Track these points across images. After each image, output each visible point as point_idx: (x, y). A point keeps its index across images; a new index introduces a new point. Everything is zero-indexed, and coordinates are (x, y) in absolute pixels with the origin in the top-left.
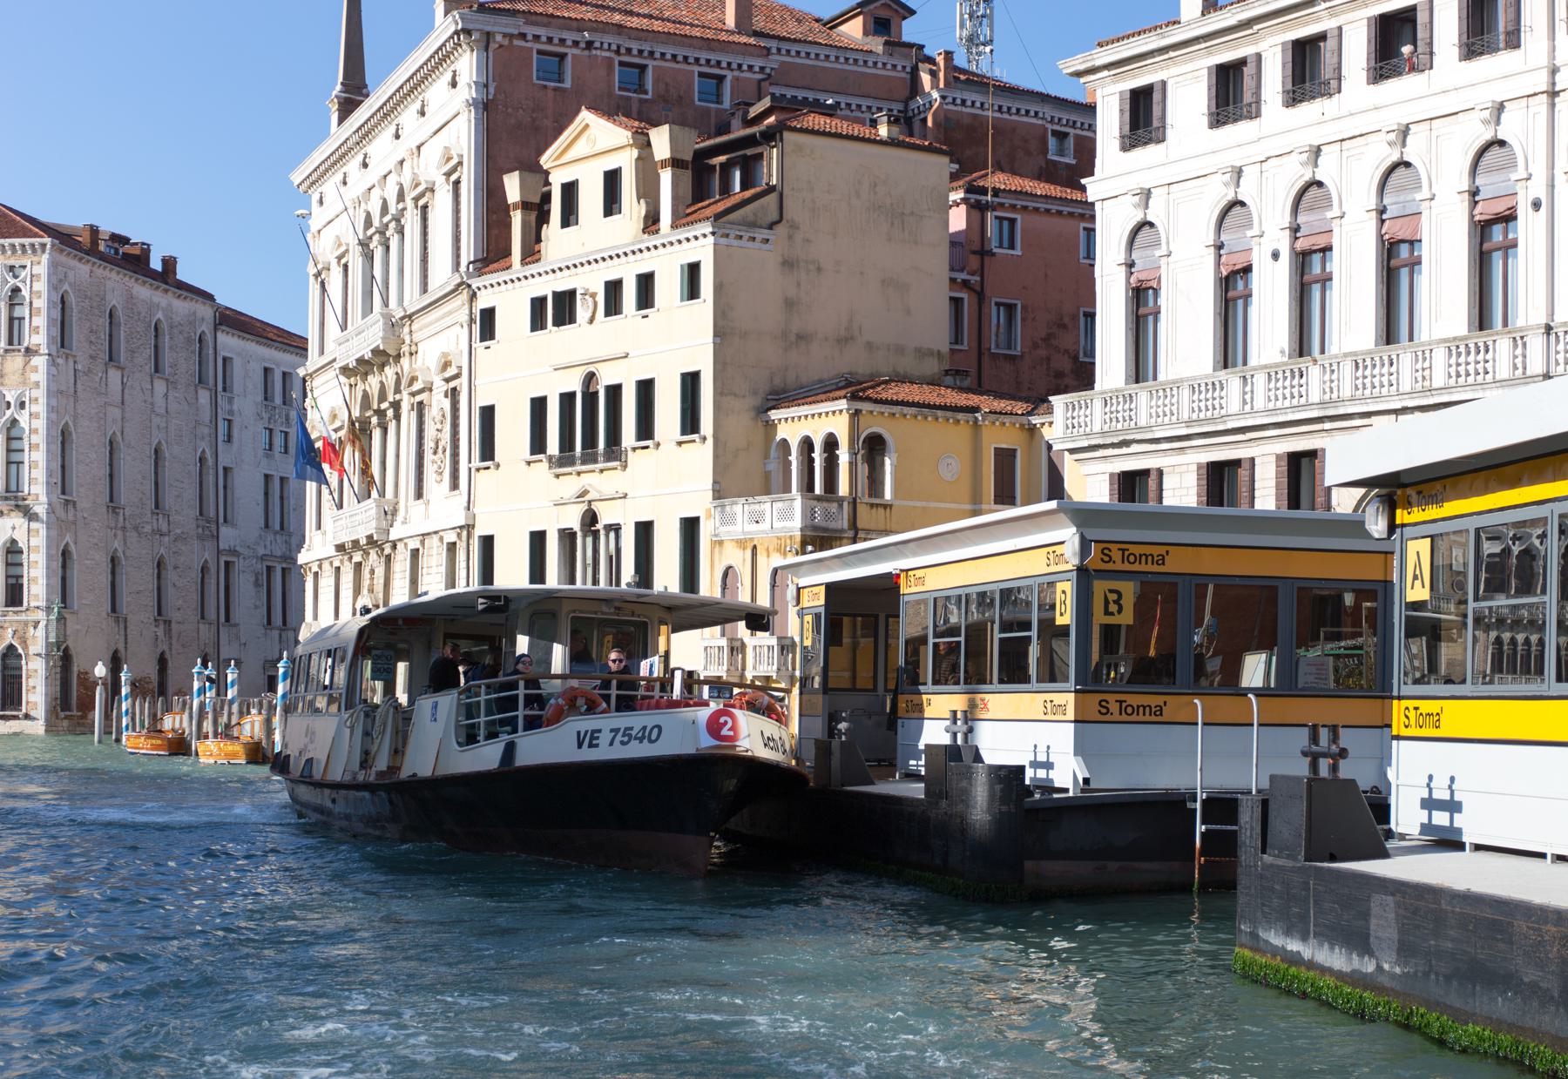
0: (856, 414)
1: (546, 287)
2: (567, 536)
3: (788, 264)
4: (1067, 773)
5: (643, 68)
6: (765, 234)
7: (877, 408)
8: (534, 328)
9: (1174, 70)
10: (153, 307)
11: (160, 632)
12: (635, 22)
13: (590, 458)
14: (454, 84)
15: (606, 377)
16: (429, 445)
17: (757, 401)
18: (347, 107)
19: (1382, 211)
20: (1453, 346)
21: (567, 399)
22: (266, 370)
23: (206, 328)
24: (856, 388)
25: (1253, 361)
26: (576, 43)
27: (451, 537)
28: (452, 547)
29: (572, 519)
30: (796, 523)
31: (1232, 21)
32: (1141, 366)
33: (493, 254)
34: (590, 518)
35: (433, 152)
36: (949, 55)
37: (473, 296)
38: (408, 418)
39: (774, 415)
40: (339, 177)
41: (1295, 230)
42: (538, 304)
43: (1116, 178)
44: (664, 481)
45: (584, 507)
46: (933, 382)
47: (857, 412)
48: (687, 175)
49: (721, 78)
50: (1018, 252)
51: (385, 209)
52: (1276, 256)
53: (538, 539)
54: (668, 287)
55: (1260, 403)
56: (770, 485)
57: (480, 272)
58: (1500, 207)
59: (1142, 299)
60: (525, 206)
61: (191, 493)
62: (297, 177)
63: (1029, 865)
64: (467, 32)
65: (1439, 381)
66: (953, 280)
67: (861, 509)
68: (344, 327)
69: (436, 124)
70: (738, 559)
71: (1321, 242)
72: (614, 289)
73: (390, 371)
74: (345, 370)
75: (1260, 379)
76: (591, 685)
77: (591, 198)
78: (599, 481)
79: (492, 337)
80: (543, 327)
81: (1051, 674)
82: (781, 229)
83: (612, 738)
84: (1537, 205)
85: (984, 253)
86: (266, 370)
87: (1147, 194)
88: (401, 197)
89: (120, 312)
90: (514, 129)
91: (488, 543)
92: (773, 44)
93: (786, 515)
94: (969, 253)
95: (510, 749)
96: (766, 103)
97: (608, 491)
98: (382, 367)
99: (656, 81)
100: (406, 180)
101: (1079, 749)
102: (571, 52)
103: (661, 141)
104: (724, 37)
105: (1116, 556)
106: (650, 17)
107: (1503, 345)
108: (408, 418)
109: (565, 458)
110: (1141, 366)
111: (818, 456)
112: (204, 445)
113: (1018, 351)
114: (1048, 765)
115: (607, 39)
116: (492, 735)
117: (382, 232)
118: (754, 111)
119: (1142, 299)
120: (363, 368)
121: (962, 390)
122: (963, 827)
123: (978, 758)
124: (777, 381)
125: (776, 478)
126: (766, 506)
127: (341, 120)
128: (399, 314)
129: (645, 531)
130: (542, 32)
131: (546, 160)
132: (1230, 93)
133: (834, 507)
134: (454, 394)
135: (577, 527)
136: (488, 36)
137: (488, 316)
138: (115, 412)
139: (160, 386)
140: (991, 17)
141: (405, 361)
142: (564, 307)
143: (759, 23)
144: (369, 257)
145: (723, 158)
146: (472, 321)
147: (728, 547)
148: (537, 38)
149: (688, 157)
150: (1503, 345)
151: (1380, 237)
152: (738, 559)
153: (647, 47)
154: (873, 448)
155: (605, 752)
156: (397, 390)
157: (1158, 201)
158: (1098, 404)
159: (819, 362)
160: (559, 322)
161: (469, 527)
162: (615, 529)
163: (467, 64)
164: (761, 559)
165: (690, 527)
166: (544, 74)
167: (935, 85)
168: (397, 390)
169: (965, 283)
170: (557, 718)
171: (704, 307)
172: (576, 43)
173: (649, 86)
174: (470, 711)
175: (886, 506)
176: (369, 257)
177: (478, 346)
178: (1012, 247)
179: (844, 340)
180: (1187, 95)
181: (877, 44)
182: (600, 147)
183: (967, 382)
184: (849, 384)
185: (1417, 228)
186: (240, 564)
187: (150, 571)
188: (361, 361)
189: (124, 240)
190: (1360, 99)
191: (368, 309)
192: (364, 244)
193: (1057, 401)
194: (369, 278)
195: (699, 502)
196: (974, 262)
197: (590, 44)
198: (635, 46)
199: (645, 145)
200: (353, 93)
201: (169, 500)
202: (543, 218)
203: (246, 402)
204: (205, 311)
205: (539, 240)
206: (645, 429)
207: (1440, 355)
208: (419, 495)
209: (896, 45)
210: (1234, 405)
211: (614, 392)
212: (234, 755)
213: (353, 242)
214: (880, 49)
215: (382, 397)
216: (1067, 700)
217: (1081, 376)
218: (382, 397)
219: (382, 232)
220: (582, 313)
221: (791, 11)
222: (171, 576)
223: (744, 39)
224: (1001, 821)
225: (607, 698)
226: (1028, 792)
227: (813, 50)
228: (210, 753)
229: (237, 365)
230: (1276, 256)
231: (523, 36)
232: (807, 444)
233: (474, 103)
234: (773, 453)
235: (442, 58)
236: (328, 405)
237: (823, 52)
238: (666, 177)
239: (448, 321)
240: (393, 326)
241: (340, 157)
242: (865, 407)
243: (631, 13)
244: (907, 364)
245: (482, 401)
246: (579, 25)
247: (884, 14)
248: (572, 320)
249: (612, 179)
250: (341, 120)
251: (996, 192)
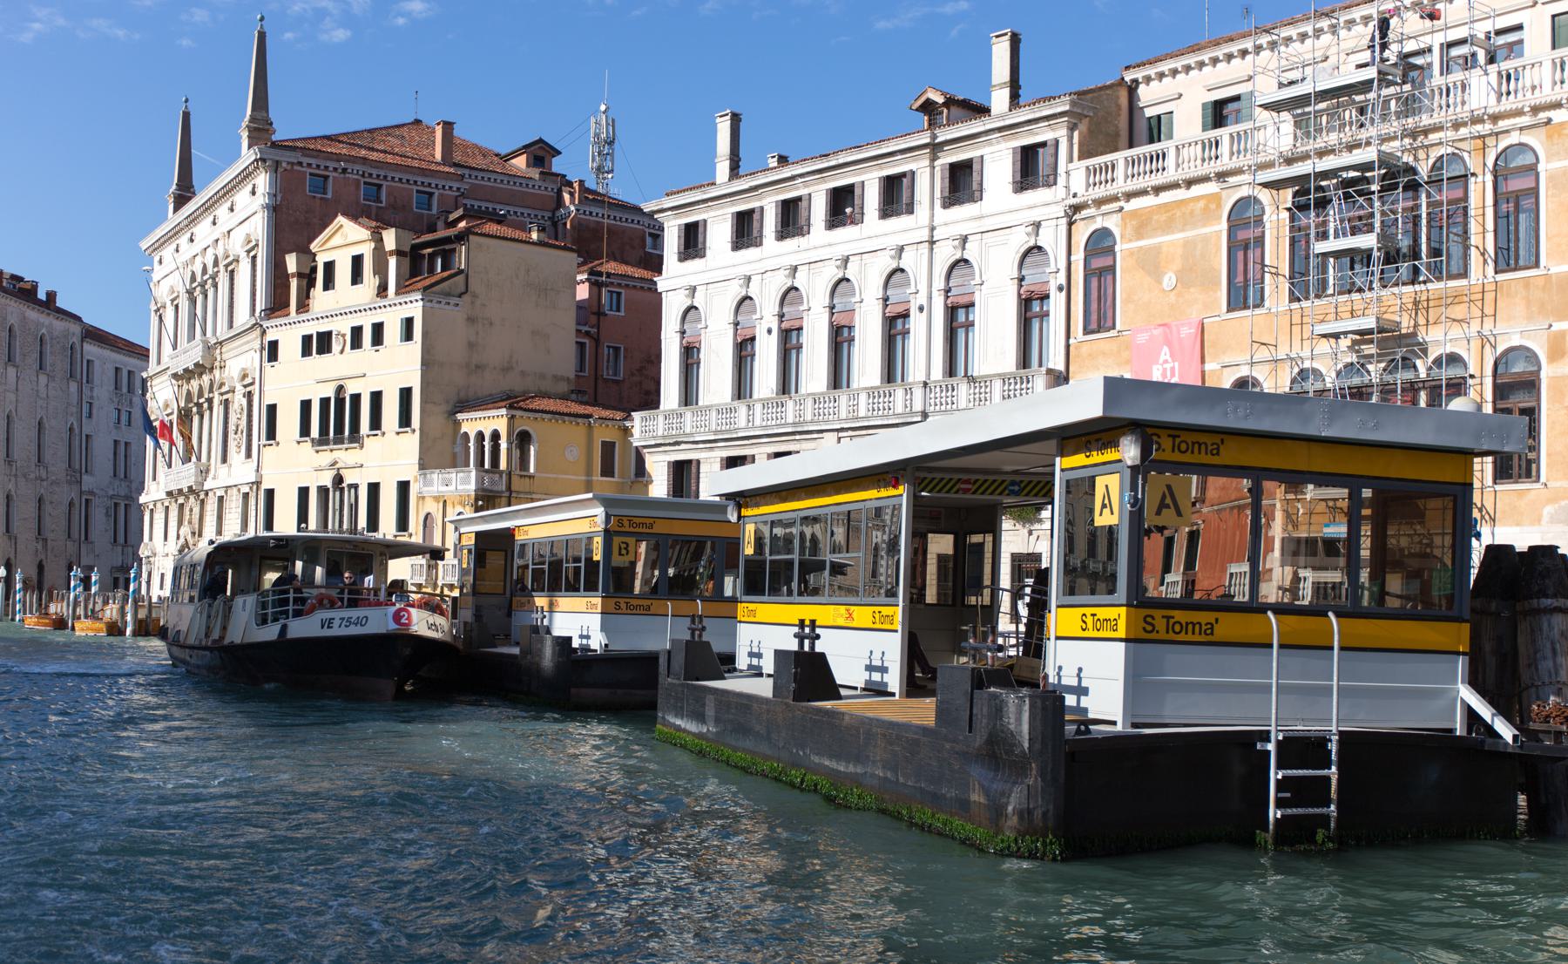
0: (511, 418)
1: (313, 328)
2: (323, 491)
3: (471, 320)
4: (597, 642)
5: (380, 186)
6: (456, 300)
7: (526, 414)
8: (304, 355)
9: (712, 214)
10: (39, 325)
11: (40, 547)
12: (374, 156)
13: (339, 440)
14: (254, 193)
15: (351, 388)
16: (232, 428)
17: (450, 408)
18: (181, 201)
19: (832, 307)
20: (871, 392)
21: (325, 402)
22: (117, 369)
23: (76, 340)
24: (512, 401)
25: (755, 396)
26: (335, 169)
27: (246, 489)
28: (246, 496)
29: (327, 480)
30: (472, 486)
31: (746, 186)
32: (688, 395)
33: (278, 305)
34: (338, 480)
35: (238, 237)
36: (581, 182)
37: (264, 333)
38: (218, 410)
39: (460, 416)
40: (174, 246)
41: (781, 316)
42: (307, 340)
43: (675, 278)
44: (388, 457)
45: (333, 473)
46: (564, 398)
47: (513, 417)
48: (407, 261)
49: (431, 195)
50: (622, 314)
52: (769, 331)
53: (304, 493)
54: (392, 332)
55: (758, 422)
56: (456, 461)
57: (268, 317)
58: (900, 309)
59: (690, 354)
60: (300, 275)
61: (63, 452)
62: (144, 245)
63: (573, 690)
64: (263, 160)
65: (862, 413)
66: (578, 331)
67: (514, 478)
68: (175, 348)
69: (241, 218)
70: (434, 508)
71: (796, 324)
72: (357, 332)
73: (206, 378)
74: (175, 376)
75: (758, 407)
76: (334, 593)
77: (343, 272)
78: (345, 456)
79: (276, 359)
80: (310, 354)
81: (591, 587)
82: (466, 298)
83: (341, 623)
84: (921, 309)
85: (599, 314)
86: (117, 369)
87: (693, 290)
88: (216, 263)
89: (16, 328)
90: (293, 225)
91: (270, 494)
92: (467, 172)
93: (466, 481)
94: (589, 313)
95: (284, 628)
96: (460, 212)
97: (351, 462)
98: (200, 375)
99: (388, 195)
100: (220, 252)
101: (603, 628)
102: (332, 174)
103: (390, 239)
104: (433, 167)
105: (626, 523)
106: (385, 152)
107: (900, 393)
108: (218, 410)
109: (323, 440)
110: (688, 395)
111: (487, 443)
112: (73, 420)
113: (621, 378)
114: (588, 637)
115: (357, 167)
116: (275, 620)
117: (203, 285)
118: (452, 217)
119: (690, 354)
120: (188, 375)
121: (582, 403)
122: (539, 669)
123: (548, 631)
124: (462, 395)
125: (460, 458)
126: (453, 475)
127: (176, 210)
128: (213, 341)
129: (374, 489)
130: (314, 162)
131: (314, 247)
132: (745, 230)
133: (496, 477)
134: (249, 396)
135: (329, 485)
136: (277, 163)
137: (274, 346)
138: (12, 397)
139: (43, 379)
140: (612, 155)
141: (217, 372)
142: (324, 343)
143: (457, 157)
144: (193, 301)
145: (430, 250)
146: (262, 348)
147: (423, 502)
148: (309, 165)
149: (407, 249)
150: (900, 393)
151: (831, 323)
152: (434, 508)
153: (382, 173)
154: (522, 440)
155: (337, 631)
156: (211, 391)
157: (702, 292)
158: (661, 418)
159: (490, 383)
160: (321, 351)
161: (258, 483)
162: (356, 487)
163: (262, 180)
164: (449, 509)
165: (404, 487)
166: (314, 189)
167: (572, 202)
168: (211, 391)
169: (587, 334)
170: (312, 610)
171: (415, 347)
172: (335, 169)
173: (384, 198)
174: (264, 606)
175: (531, 477)
176: (193, 301)
177: (266, 365)
178: (618, 310)
179: (507, 369)
180: (719, 232)
181: (535, 173)
182: (349, 240)
183: (586, 398)
184: (509, 398)
185: (852, 319)
186: (95, 501)
187: (33, 505)
188: (186, 370)
189: (20, 279)
190: (820, 238)
191: (192, 337)
192: (190, 292)
193: (636, 415)
194: (193, 315)
195: (410, 472)
196: (593, 319)
197: (344, 170)
198: (375, 172)
199: (379, 240)
200: (184, 194)
201: (47, 457)
202: (312, 283)
203: (102, 391)
204: (76, 329)
205: (308, 297)
206: (376, 423)
207: (863, 397)
208: (224, 460)
209: (548, 175)
210: (742, 422)
211: (356, 398)
212: (99, 630)
213: (182, 291)
214: (537, 176)
215: (200, 395)
216: (598, 601)
217: (651, 400)
218: (200, 395)
219: (203, 285)
220: (336, 347)
221: (480, 149)
222: (48, 508)
223: (447, 169)
224: (558, 666)
225: (342, 600)
226: (575, 650)
227: (493, 177)
228: (84, 629)
229: (97, 364)
230: (769, 331)
231: (300, 164)
232: (480, 436)
233: (267, 207)
234: (459, 441)
235: (245, 176)
236: (162, 397)
237: (499, 178)
238: (392, 262)
239: (246, 347)
240: (209, 349)
241: (175, 233)
242: (518, 413)
243: (373, 149)
244: (547, 386)
245: (268, 401)
246: (338, 157)
247: (541, 153)
248: (329, 351)
249: (357, 261)
250: (176, 210)
251: (609, 275)
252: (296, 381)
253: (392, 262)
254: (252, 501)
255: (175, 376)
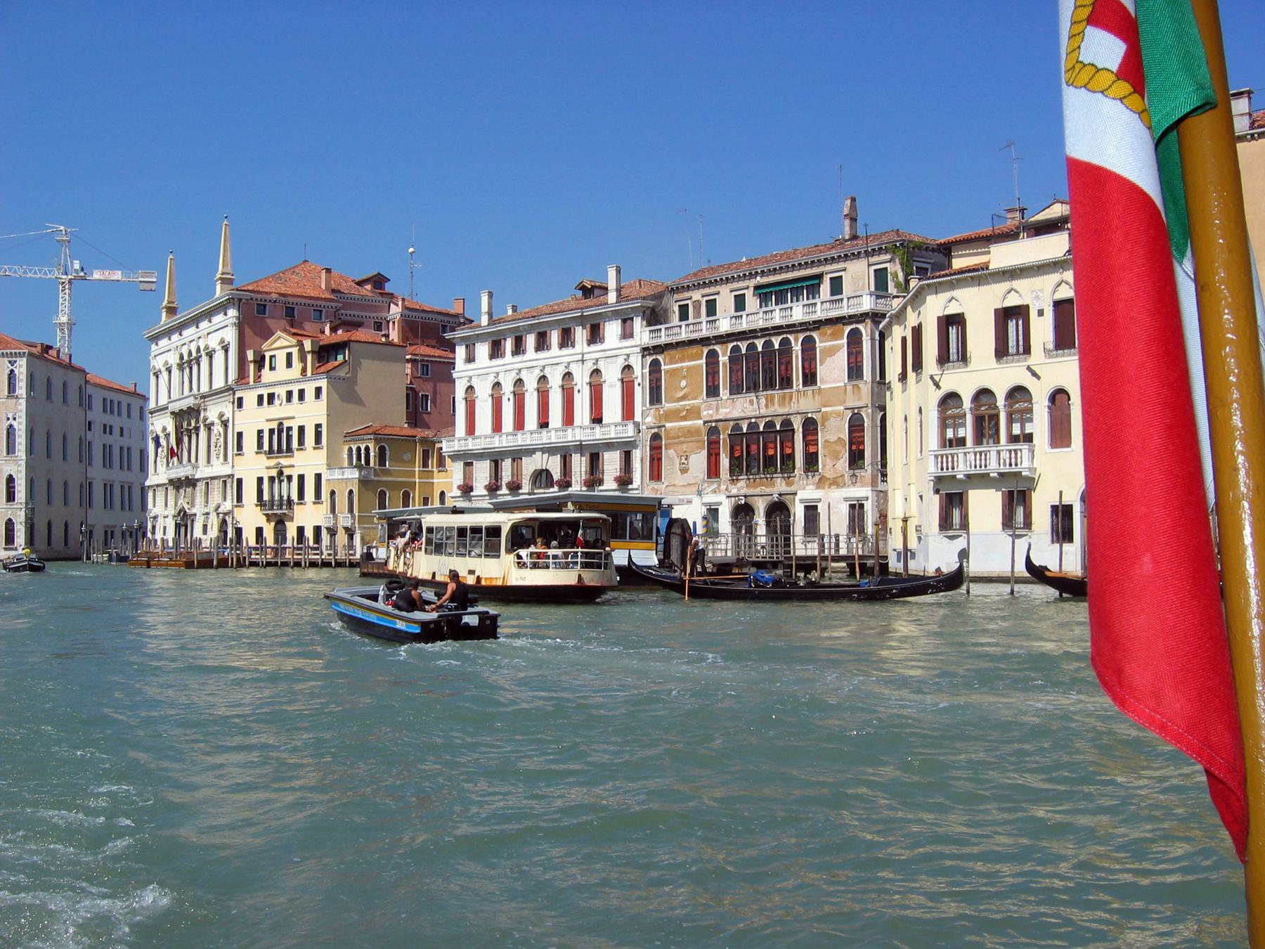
1: (265, 392)
2: (272, 479)
15: (286, 424)
21: (271, 431)
28: (225, 482)
29: (274, 473)
34: (281, 473)
38: (203, 433)
42: (260, 398)
51: (190, 353)
60: (255, 362)
72: (290, 394)
74: (172, 413)
78: (284, 462)
91: (240, 481)
137: (240, 400)
162: (290, 478)
208: (209, 461)
220: (277, 402)
222: (70, 489)
238: (309, 357)
245: (237, 430)
249: (289, 355)
252: (253, 419)
253: (309, 357)
254: (229, 485)
255: (172, 413)
